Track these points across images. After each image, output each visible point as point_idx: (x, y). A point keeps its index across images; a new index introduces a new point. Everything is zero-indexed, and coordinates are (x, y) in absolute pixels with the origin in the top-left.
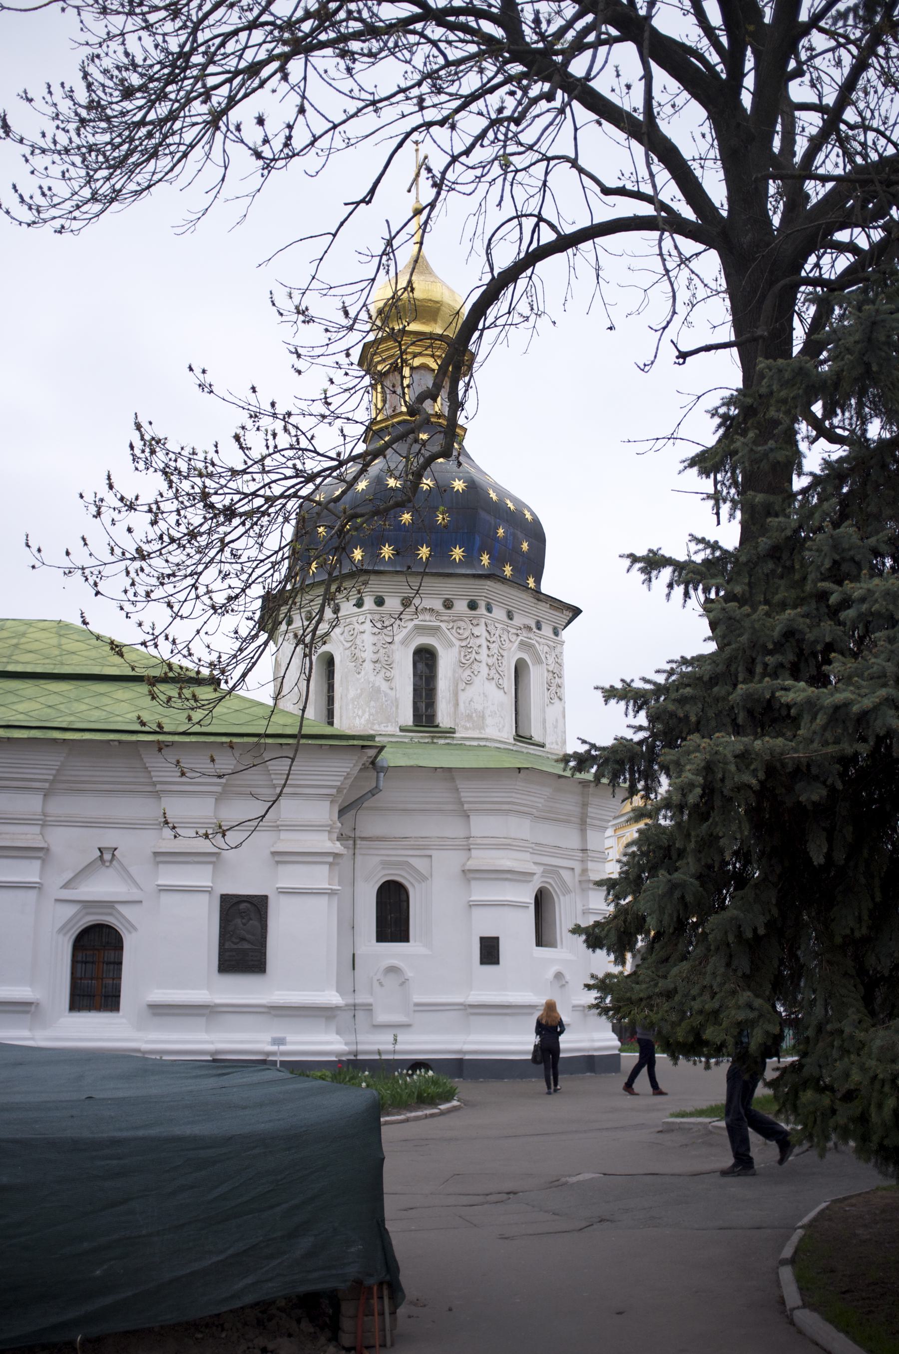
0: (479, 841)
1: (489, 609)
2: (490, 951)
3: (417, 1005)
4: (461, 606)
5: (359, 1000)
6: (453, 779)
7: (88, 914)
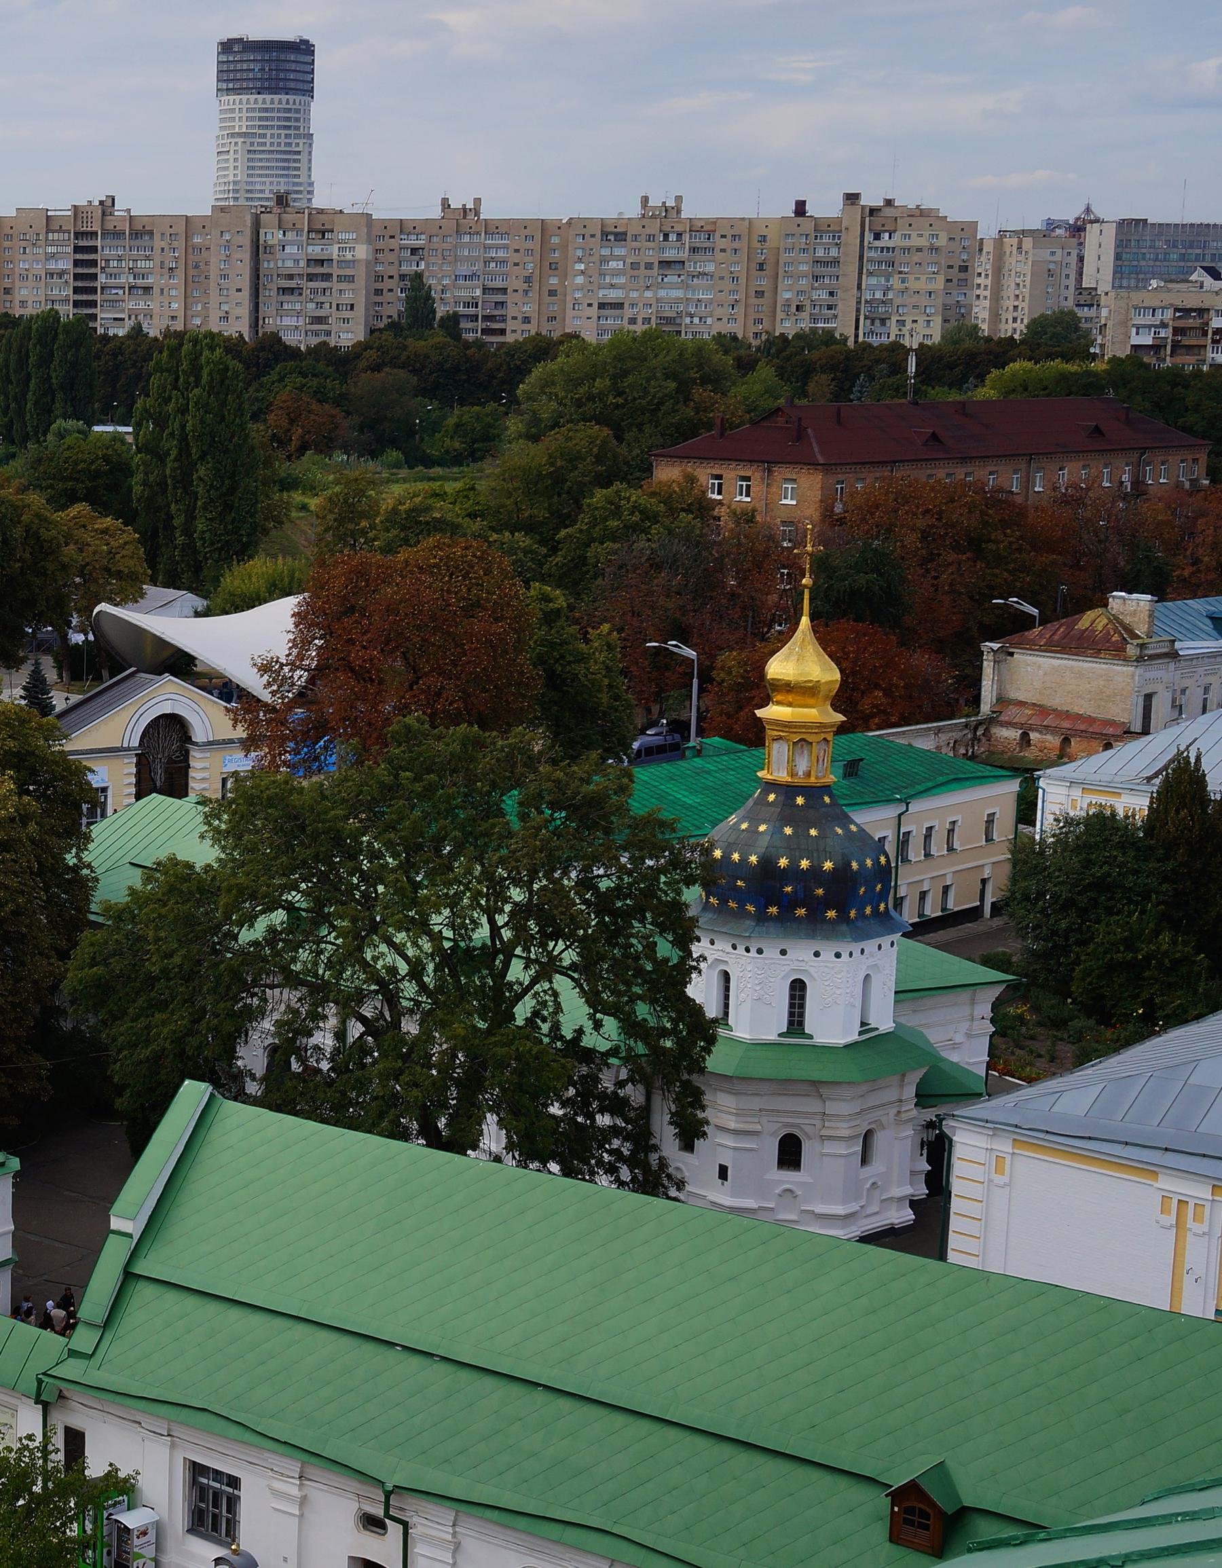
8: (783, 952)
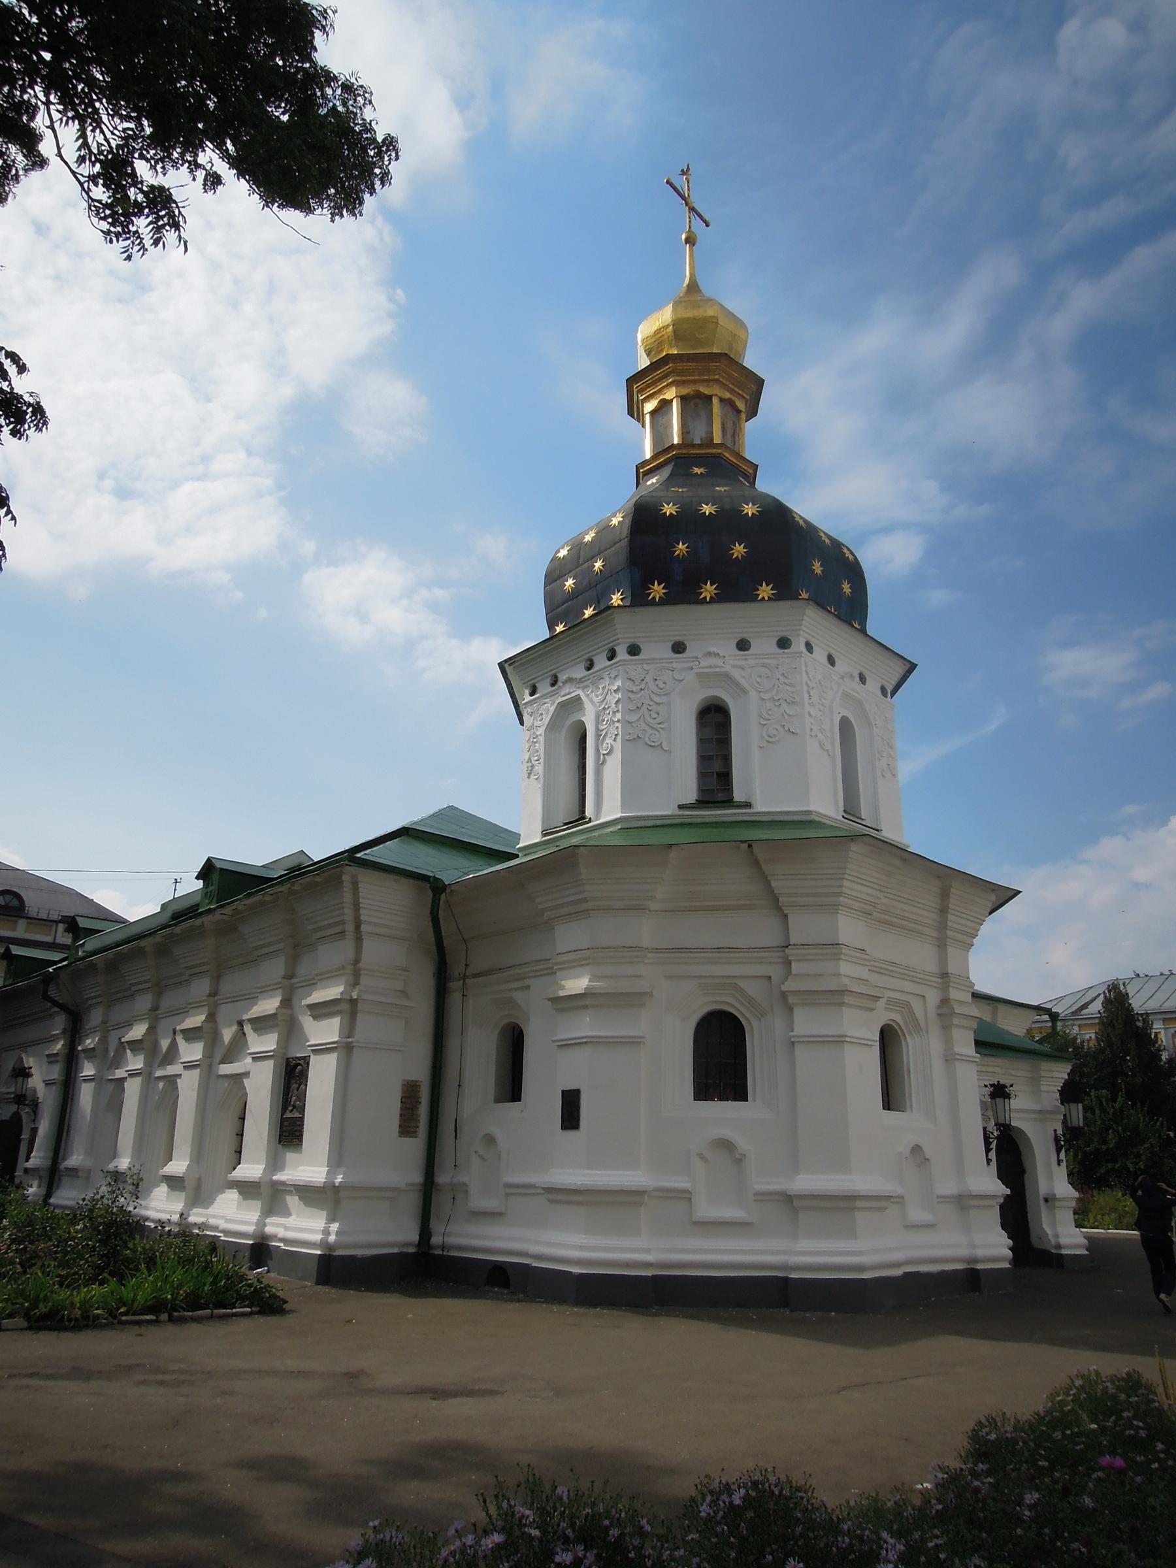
1: (634, 650)
4: (601, 662)
8: (679, 648)
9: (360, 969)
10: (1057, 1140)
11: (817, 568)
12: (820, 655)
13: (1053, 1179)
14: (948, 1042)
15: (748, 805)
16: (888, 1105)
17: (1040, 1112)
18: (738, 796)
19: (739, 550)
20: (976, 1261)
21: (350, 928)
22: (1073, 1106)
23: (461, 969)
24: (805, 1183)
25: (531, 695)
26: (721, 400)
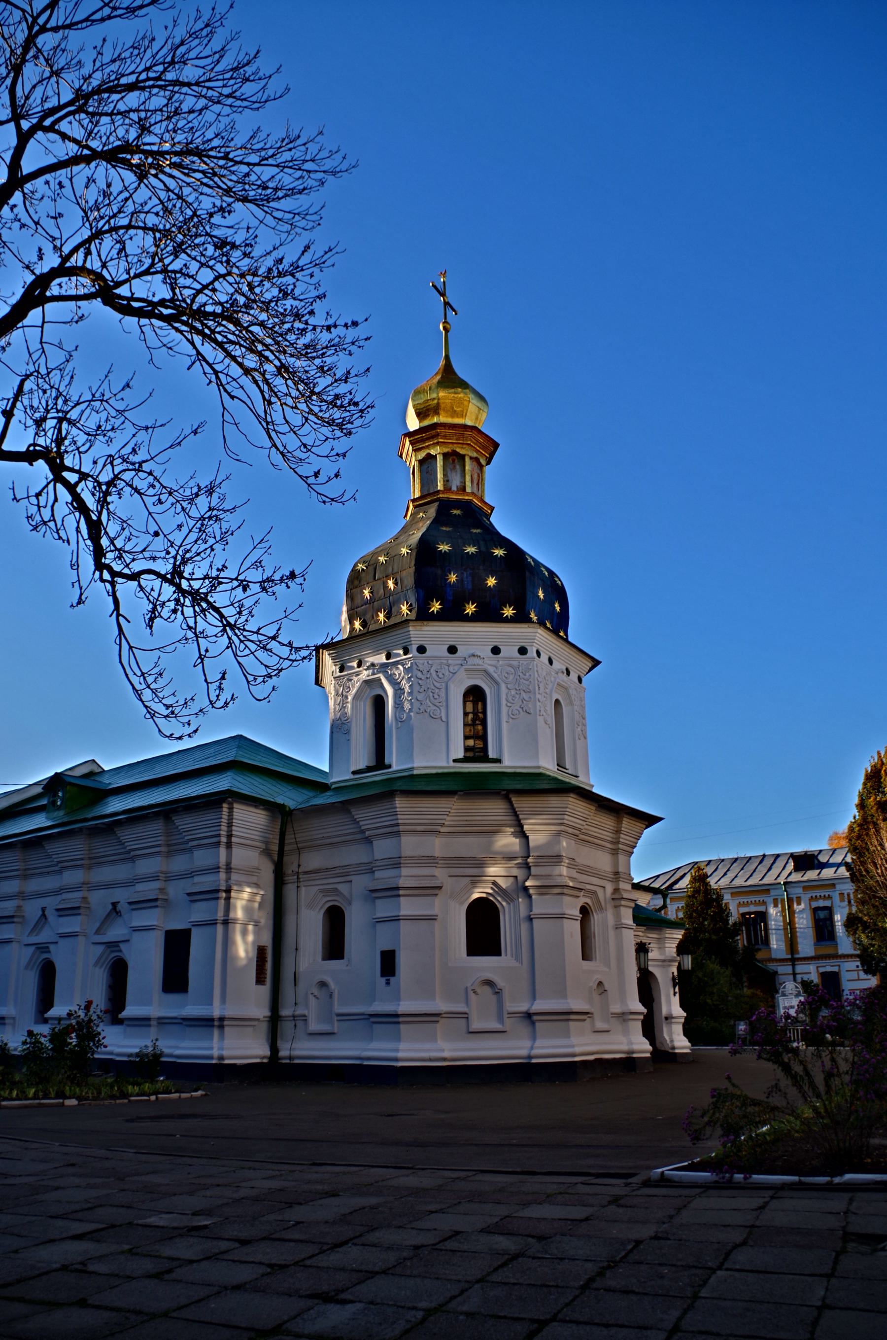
0: (378, 864)
2: (389, 963)
3: (338, 1015)
5: (299, 1012)
6: (349, 812)
7: (112, 952)
9: (231, 868)
10: (674, 979)
11: (541, 595)
12: (544, 658)
13: (672, 1005)
14: (618, 916)
15: (498, 761)
16: (583, 959)
17: (664, 961)
18: (492, 754)
19: (491, 582)
20: (633, 1052)
21: (224, 839)
22: (685, 957)
23: (294, 867)
24: (539, 1006)
25: (341, 671)
26: (471, 458)
